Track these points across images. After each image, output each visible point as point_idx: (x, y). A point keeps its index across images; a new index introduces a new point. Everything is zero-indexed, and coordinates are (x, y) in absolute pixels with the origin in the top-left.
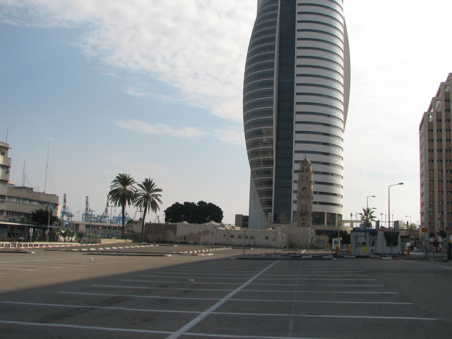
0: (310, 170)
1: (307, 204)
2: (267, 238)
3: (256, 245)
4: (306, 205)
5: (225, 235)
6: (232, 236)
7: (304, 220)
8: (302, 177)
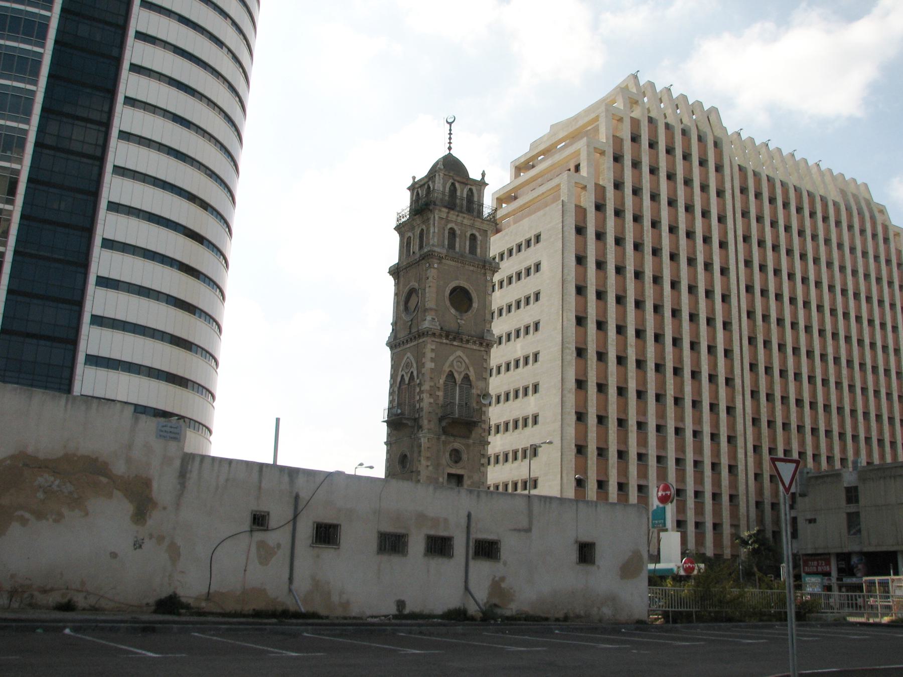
0: (481, 205)
1: (472, 377)
2: (586, 553)
3: (512, 609)
4: (467, 378)
5: (259, 521)
6: (326, 534)
7: (456, 457)
8: (452, 232)
